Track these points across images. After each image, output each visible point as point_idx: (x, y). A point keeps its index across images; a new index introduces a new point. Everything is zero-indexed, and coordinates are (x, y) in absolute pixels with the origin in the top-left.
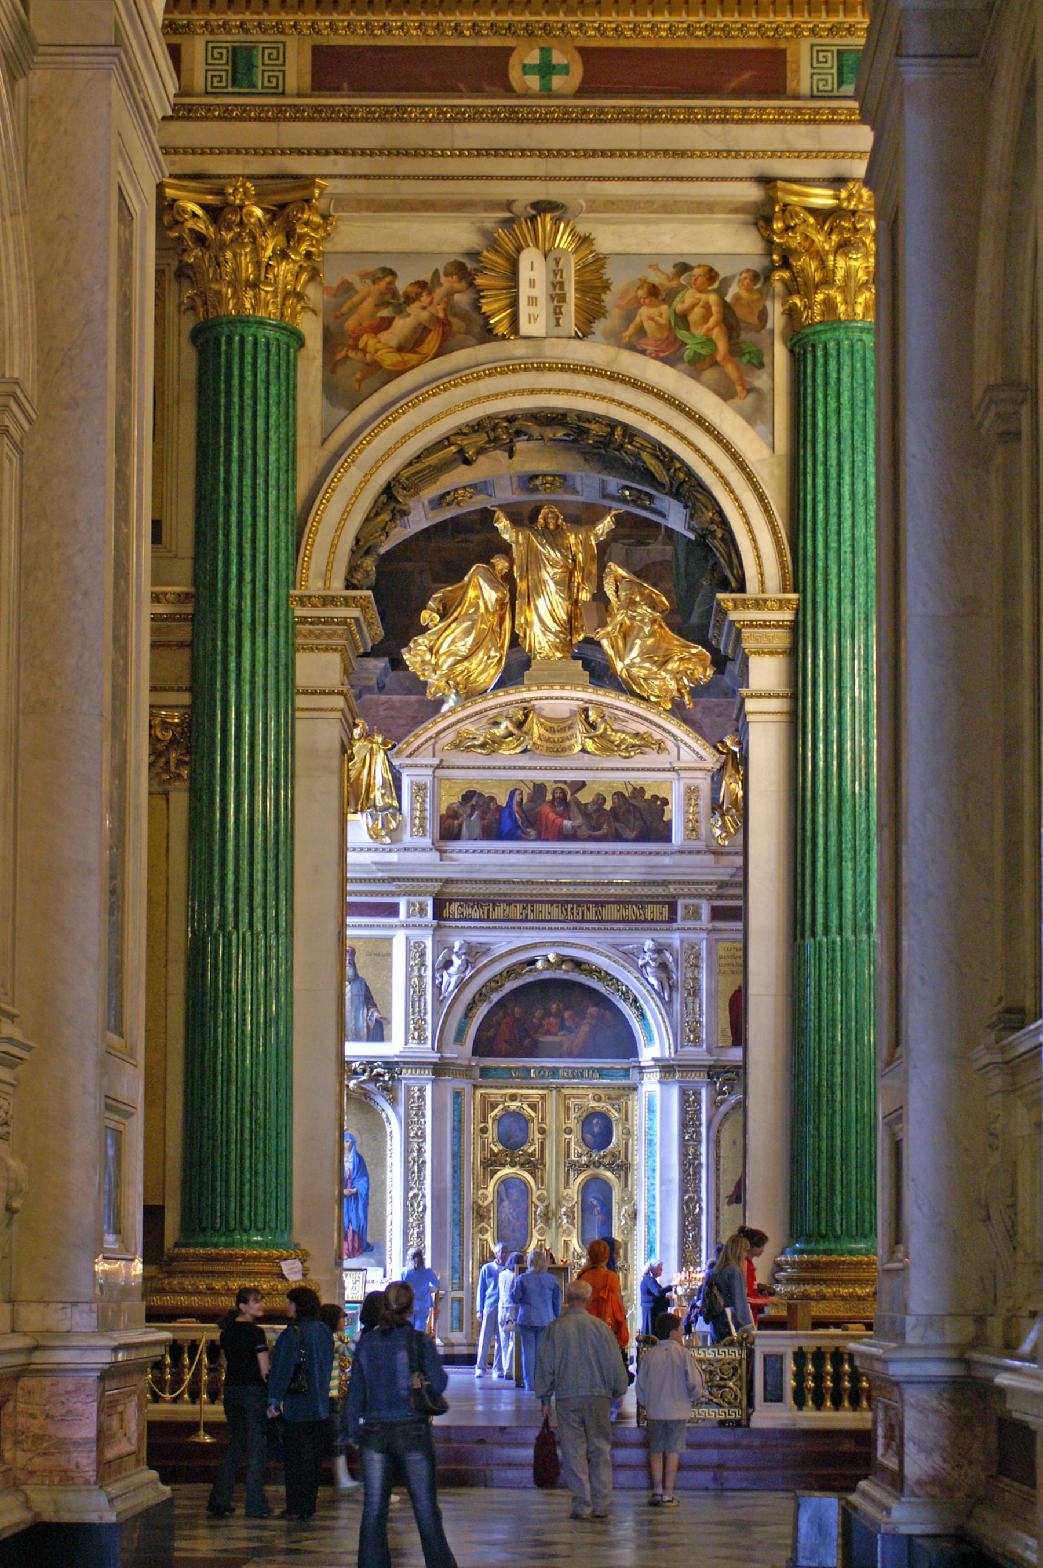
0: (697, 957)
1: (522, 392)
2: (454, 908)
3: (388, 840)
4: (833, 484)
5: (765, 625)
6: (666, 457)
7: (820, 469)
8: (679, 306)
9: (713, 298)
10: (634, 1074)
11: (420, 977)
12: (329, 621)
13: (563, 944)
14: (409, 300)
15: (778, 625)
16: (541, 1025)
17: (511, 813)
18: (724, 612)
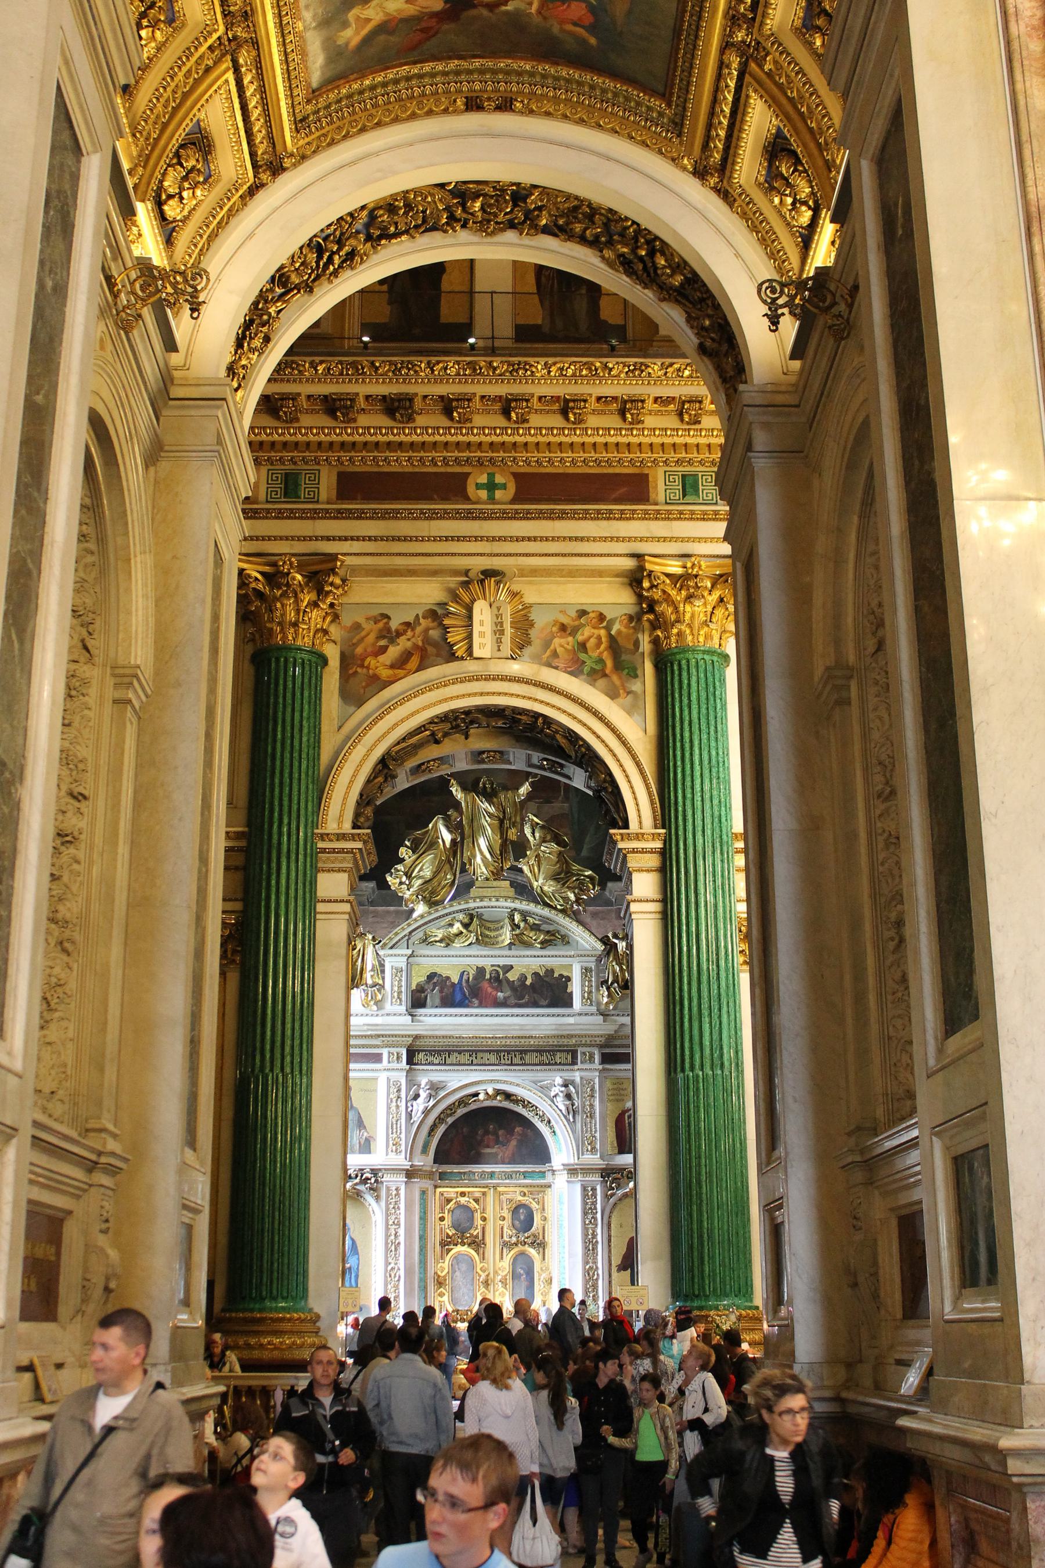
0: (593, 1090)
1: (475, 694)
2: (421, 1056)
3: (375, 1008)
4: (687, 755)
5: (643, 851)
6: (573, 737)
7: (678, 744)
8: (580, 638)
9: (603, 632)
10: (549, 1174)
11: (398, 1107)
12: (342, 851)
13: (498, 1081)
14: (399, 634)
15: (652, 851)
16: (482, 1141)
17: (461, 989)
18: (615, 843)
